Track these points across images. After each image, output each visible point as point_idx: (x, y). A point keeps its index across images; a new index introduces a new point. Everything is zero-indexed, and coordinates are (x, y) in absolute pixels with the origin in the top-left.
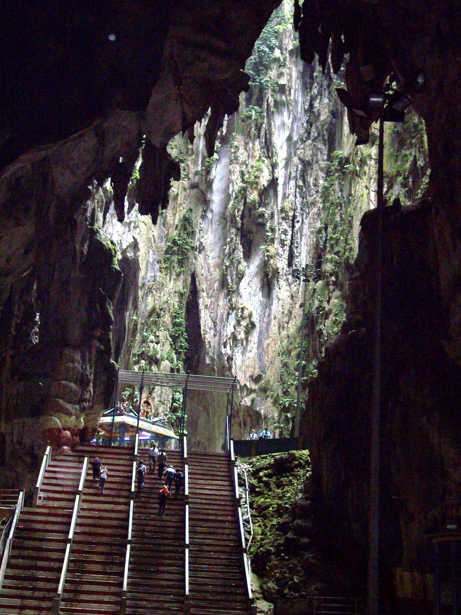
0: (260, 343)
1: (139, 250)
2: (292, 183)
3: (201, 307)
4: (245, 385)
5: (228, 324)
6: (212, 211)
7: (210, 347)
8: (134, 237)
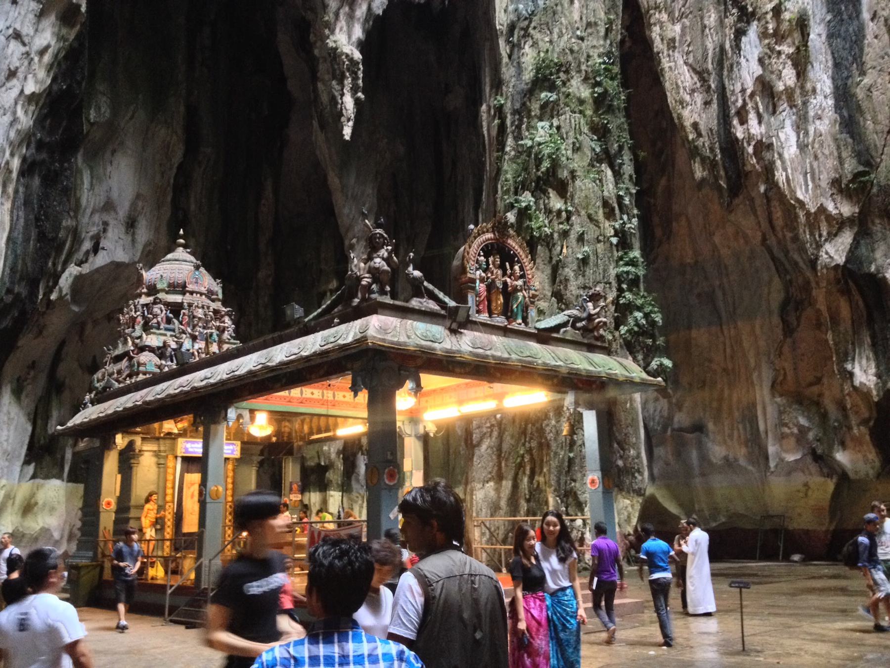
0: (844, 96)
3: (658, 45)
4: (822, 209)
5: (743, 60)
7: (700, 135)
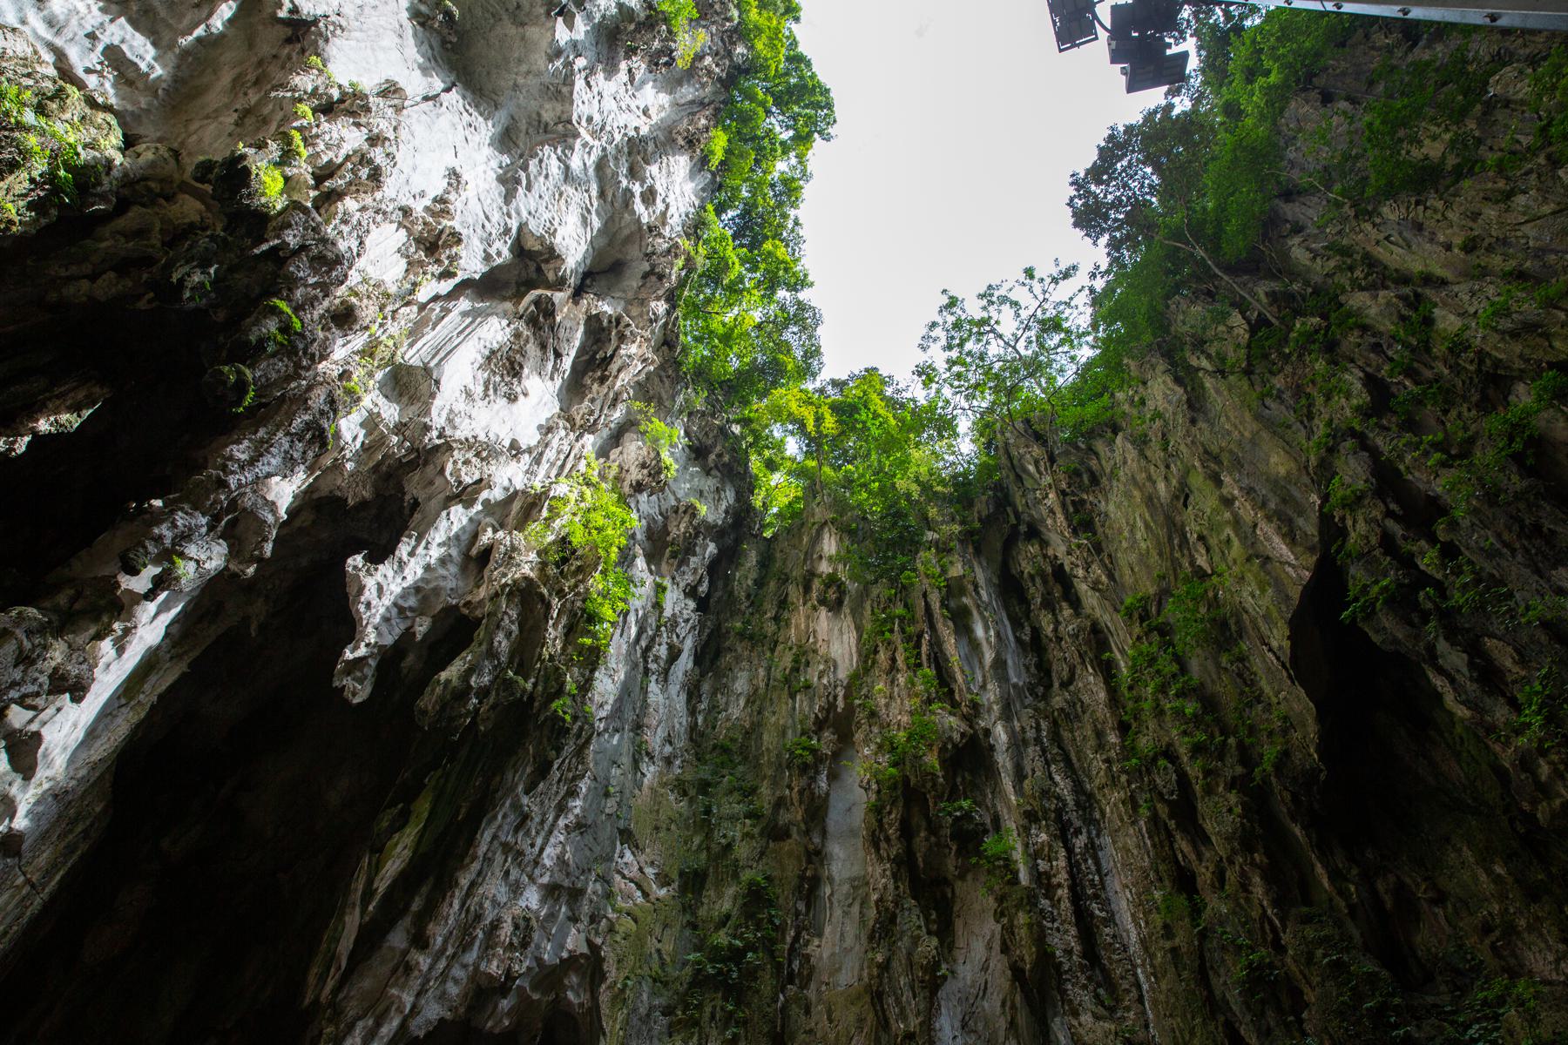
1: (603, 978)
2: (1032, 751)
6: (831, 879)
8: (589, 943)
